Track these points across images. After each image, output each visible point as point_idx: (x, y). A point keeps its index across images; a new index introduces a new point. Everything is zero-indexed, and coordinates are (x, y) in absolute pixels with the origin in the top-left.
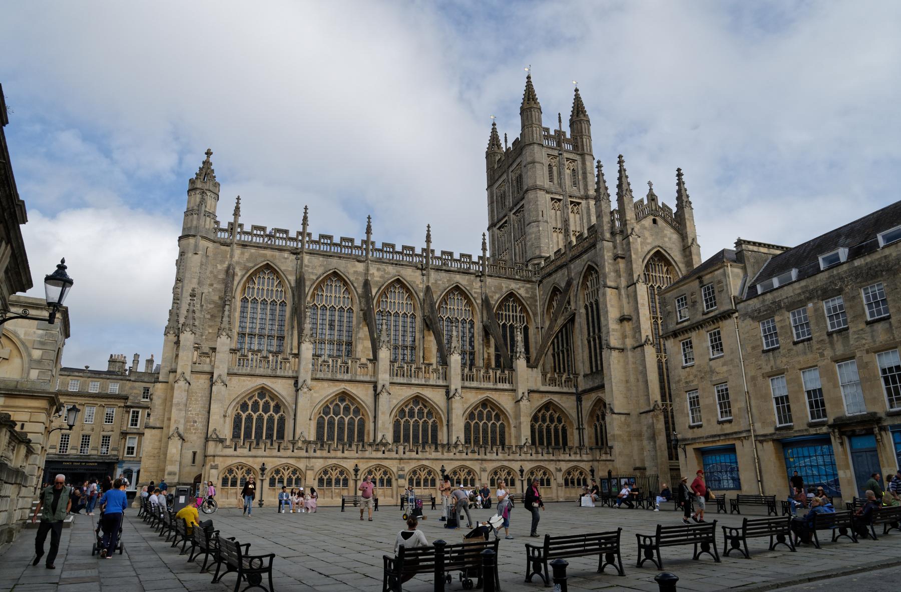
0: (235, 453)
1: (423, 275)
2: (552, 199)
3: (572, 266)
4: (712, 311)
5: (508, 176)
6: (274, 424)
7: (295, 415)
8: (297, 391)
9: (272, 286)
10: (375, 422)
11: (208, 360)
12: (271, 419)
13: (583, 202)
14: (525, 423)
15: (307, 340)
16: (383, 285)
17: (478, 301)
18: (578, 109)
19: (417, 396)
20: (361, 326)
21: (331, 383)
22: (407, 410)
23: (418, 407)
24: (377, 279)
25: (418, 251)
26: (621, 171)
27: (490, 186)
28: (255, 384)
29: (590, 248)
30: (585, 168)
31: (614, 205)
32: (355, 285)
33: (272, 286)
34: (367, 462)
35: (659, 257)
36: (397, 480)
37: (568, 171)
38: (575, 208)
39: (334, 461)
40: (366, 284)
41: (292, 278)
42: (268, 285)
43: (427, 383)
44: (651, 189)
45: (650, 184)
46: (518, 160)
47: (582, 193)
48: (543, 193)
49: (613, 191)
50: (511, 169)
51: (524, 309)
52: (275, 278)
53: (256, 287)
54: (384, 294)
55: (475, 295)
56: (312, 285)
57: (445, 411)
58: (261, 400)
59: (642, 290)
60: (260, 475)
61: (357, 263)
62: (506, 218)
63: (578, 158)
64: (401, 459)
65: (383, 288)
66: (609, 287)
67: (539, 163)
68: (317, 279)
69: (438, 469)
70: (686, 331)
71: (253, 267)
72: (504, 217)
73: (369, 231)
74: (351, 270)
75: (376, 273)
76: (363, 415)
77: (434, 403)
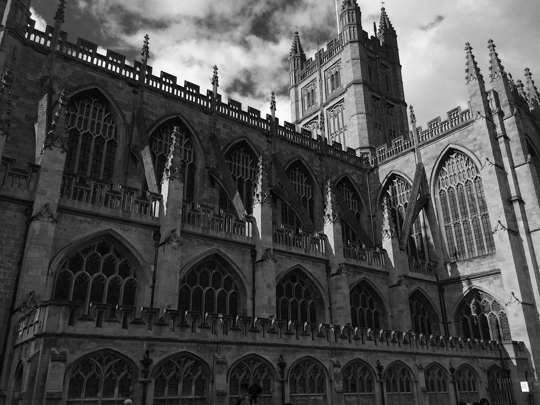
0: (99, 331)
1: (269, 142)
2: (373, 97)
3: (422, 151)
6: (118, 293)
7: (154, 281)
8: (157, 246)
9: (99, 119)
10: (253, 299)
11: (23, 181)
12: (115, 285)
13: (396, 106)
14: (406, 312)
15: (177, 176)
16: (229, 144)
17: (318, 180)
19: (297, 269)
20: (206, 185)
21: (202, 241)
22: (284, 286)
23: (296, 284)
24: (224, 136)
28: (98, 229)
32: (201, 137)
33: (99, 119)
34: (294, 351)
36: (331, 381)
39: (252, 351)
40: (213, 138)
41: (128, 115)
42: (94, 116)
43: (307, 254)
46: (336, 59)
50: (324, 68)
51: (356, 196)
52: (104, 110)
53: (78, 115)
54: (229, 155)
55: (316, 173)
56: (151, 127)
57: (326, 290)
58: (103, 254)
60: (140, 374)
61: (202, 114)
62: (319, 113)
63: (389, 65)
64: (333, 349)
65: (230, 147)
68: (158, 121)
69: (374, 366)
71: (76, 89)
72: (316, 112)
74: (196, 121)
75: (222, 129)
76: (236, 288)
77: (316, 279)
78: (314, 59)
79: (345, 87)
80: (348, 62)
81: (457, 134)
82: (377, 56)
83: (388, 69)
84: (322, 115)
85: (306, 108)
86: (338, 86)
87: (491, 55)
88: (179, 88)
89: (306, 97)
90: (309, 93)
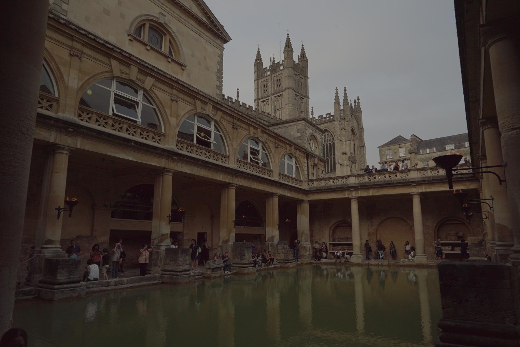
2: (296, 95)
4: (403, 157)
5: (271, 78)
13: (305, 98)
18: (303, 56)
25: (254, 109)
26: (345, 94)
27: (257, 80)
29: (327, 122)
30: (306, 83)
31: (342, 108)
35: (352, 130)
37: (301, 83)
38: (302, 100)
44: (351, 103)
45: (351, 100)
47: (304, 94)
48: (294, 91)
49: (341, 101)
50: (273, 75)
59: (352, 142)
62: (270, 98)
63: (303, 77)
66: (340, 140)
67: (292, 77)
70: (391, 162)
73: (238, 96)
78: (268, 68)
79: (284, 88)
80: (286, 77)
81: (329, 124)
82: (299, 74)
83: (303, 79)
84: (271, 99)
85: (263, 93)
86: (280, 87)
87: (344, 94)
88: (226, 99)
89: (263, 87)
90: (265, 85)
